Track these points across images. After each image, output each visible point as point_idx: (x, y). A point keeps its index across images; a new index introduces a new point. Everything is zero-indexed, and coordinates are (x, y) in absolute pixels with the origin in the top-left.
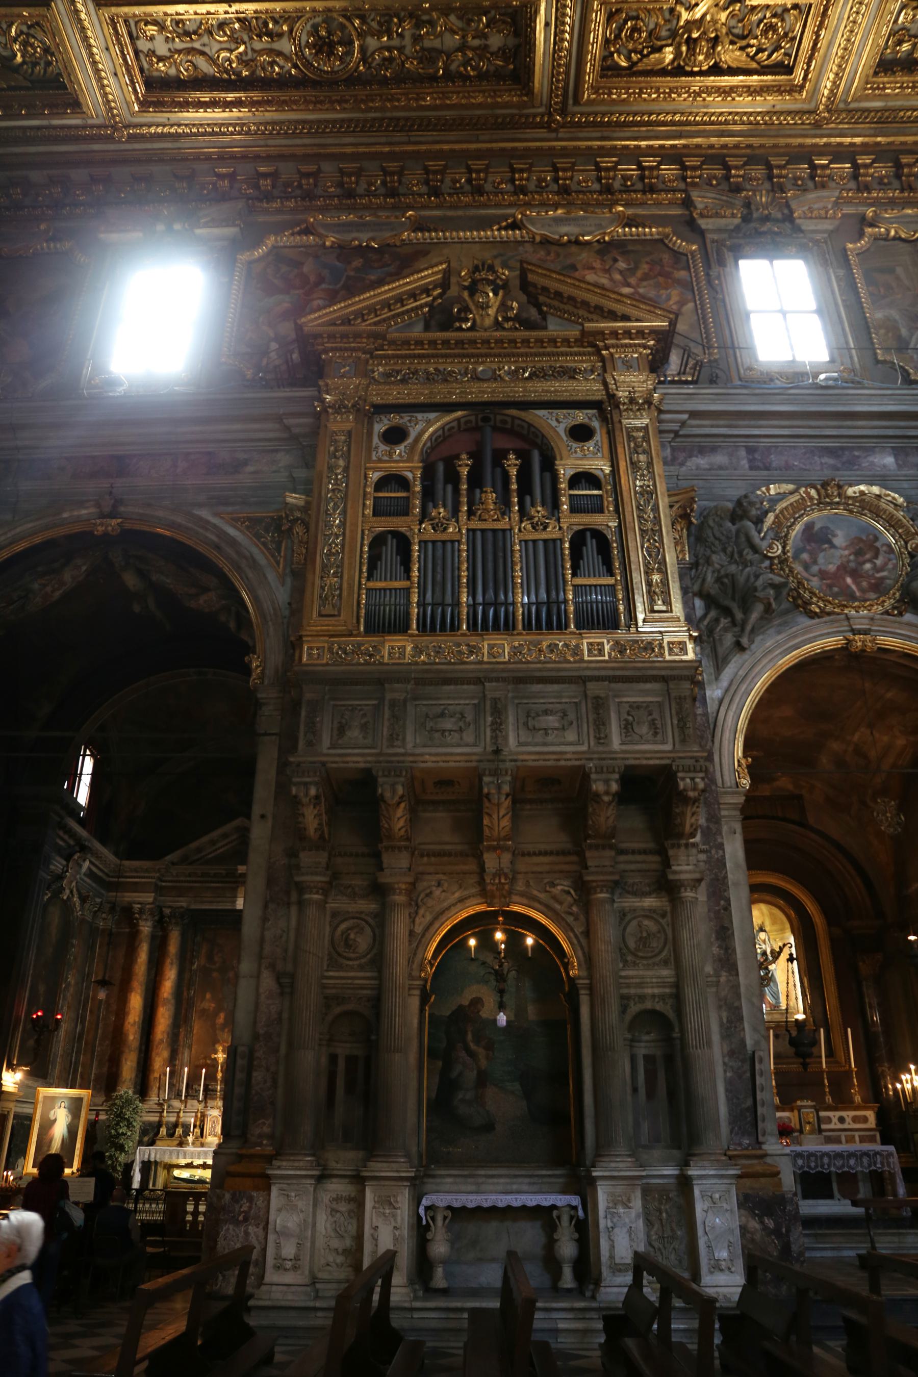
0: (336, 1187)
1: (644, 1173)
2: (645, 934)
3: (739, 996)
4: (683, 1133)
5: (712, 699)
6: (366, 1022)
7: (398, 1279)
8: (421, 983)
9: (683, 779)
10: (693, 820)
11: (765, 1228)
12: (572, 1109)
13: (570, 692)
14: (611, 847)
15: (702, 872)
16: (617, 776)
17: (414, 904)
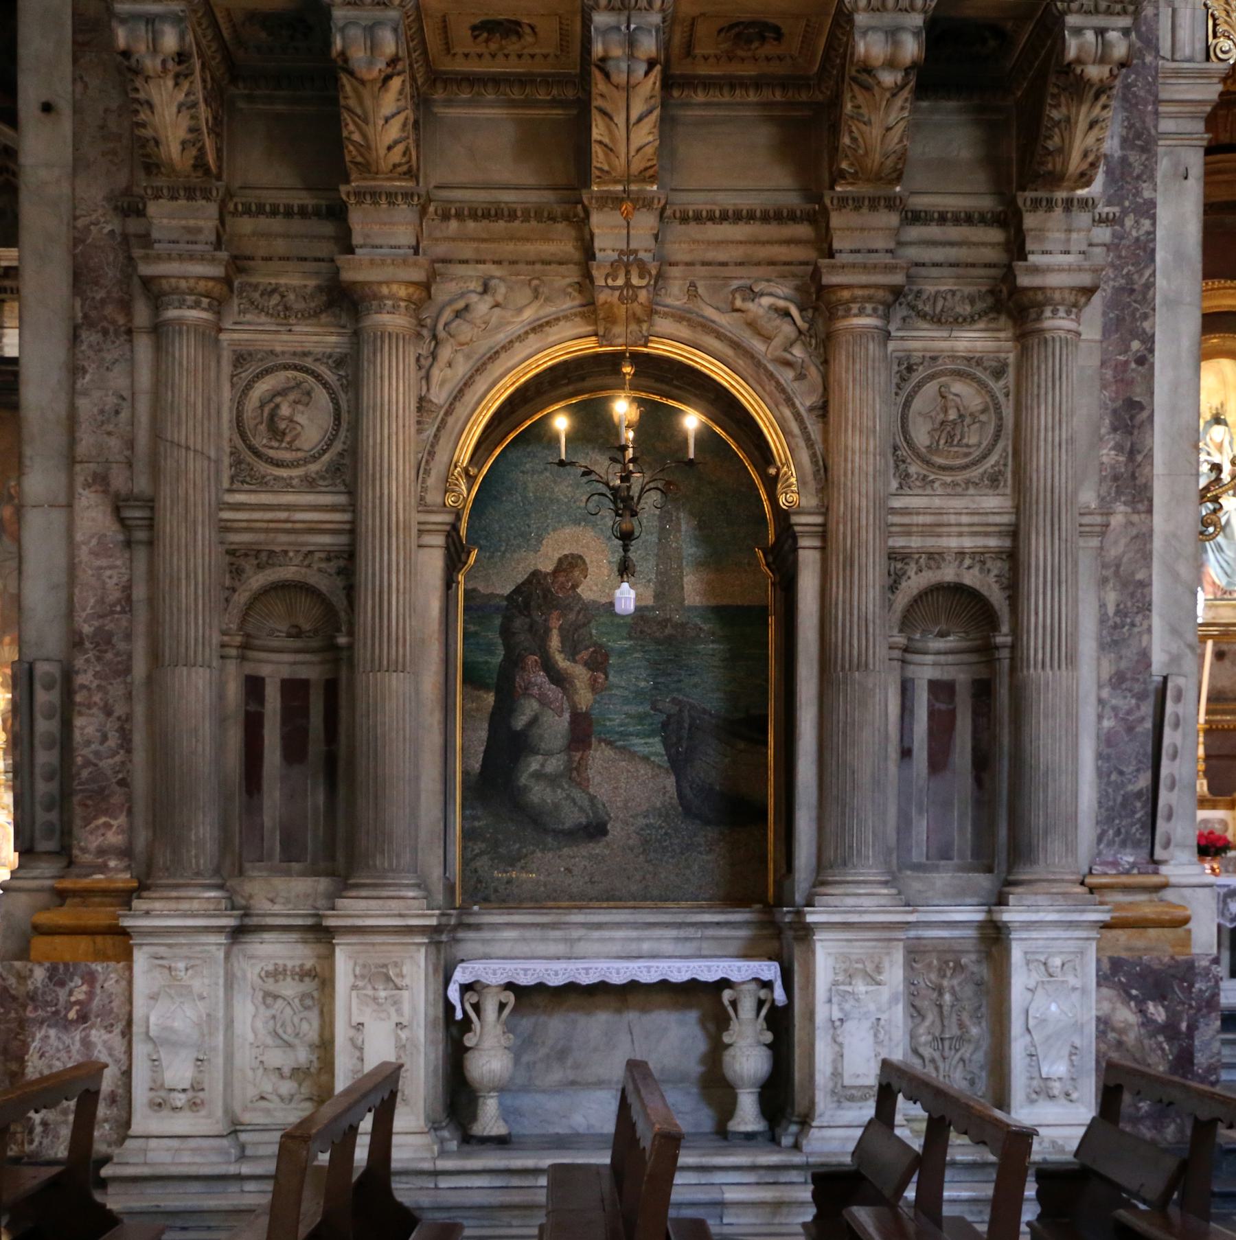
0: (272, 950)
1: (911, 918)
2: (952, 415)
3: (1146, 557)
4: (1000, 834)
6: (328, 608)
7: (409, 1121)
8: (448, 518)
9: (1078, 31)
10: (1090, 140)
11: (1147, 1022)
12: (771, 791)
14: (891, 203)
15: (1096, 271)
16: (917, 20)
17: (429, 336)
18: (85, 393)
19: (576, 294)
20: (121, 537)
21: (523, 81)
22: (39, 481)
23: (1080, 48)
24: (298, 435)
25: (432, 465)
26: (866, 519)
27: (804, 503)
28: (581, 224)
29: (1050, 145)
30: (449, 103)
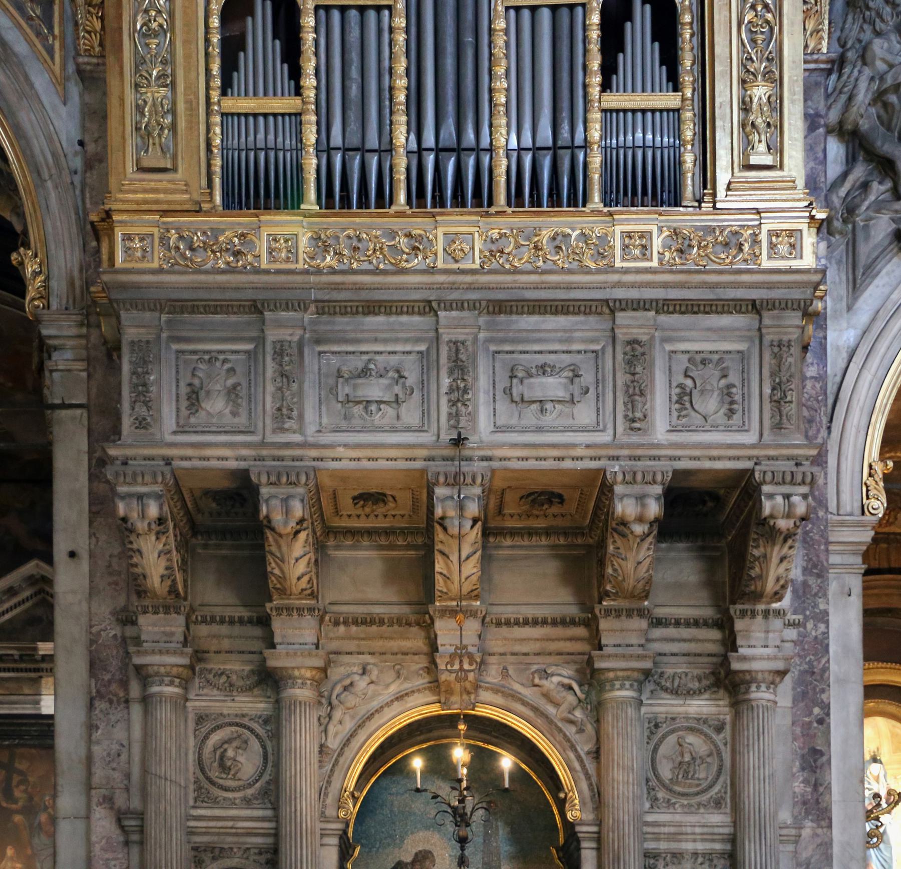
2: (687, 758)
5: (838, 348)
8: (340, 826)
9: (771, 496)
10: (781, 570)
13: (586, 329)
14: (641, 613)
15: (787, 659)
16: (658, 489)
17: (327, 704)
18: (98, 742)
19: (425, 675)
20: (121, 839)
21: (388, 532)
22: (68, 801)
23: (773, 508)
24: (239, 770)
25: (329, 789)
26: (628, 829)
27: (584, 817)
28: (428, 627)
29: (753, 573)
30: (337, 547)
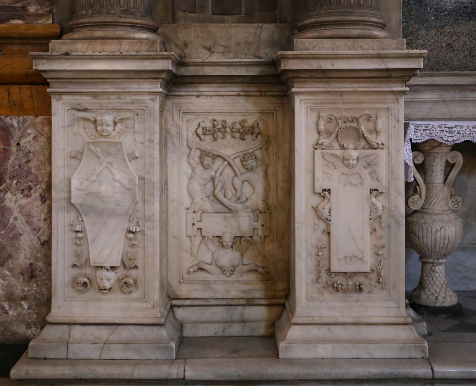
0: (212, 105)
